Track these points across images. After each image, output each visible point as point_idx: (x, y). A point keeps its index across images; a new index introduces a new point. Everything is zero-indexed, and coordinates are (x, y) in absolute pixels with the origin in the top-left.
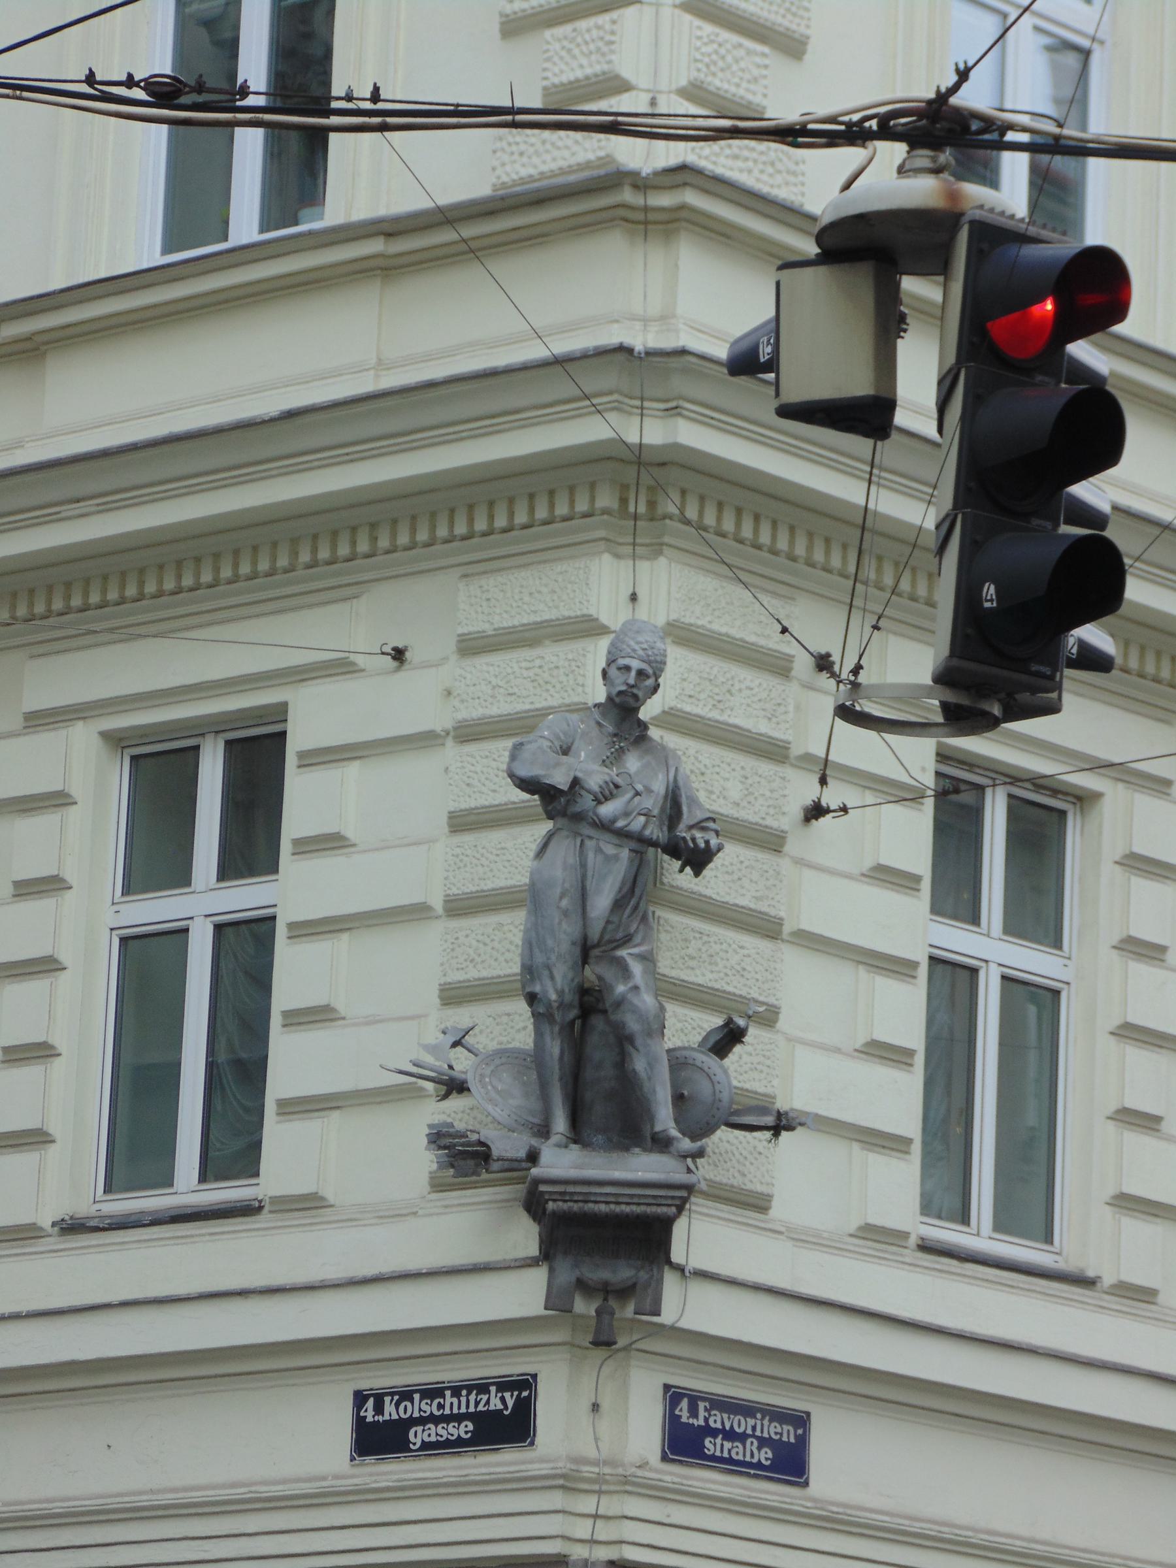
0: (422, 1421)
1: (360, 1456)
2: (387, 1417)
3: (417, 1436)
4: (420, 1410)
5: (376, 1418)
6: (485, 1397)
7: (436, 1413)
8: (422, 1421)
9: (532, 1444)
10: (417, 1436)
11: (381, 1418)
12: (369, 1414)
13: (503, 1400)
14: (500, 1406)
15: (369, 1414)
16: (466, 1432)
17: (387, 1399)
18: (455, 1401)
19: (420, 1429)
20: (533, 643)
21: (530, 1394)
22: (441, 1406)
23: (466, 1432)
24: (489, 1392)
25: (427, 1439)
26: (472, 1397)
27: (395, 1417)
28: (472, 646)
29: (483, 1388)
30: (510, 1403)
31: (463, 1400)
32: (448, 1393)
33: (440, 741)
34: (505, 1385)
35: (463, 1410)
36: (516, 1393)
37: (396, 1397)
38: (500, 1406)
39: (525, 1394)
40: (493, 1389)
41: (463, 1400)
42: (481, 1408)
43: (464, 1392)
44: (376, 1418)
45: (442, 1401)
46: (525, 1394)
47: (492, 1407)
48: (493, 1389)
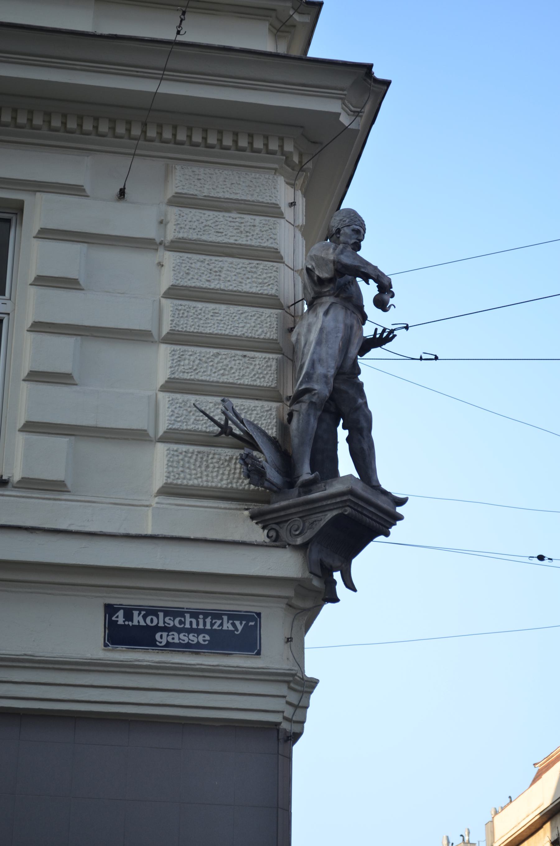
0: (166, 629)
1: (112, 644)
2: (135, 623)
3: (162, 638)
4: (164, 622)
5: (127, 623)
6: (219, 622)
7: (178, 625)
8: (166, 629)
9: (259, 653)
10: (162, 638)
11: (130, 623)
12: (120, 618)
13: (234, 625)
14: (231, 628)
15: (120, 618)
16: (204, 641)
17: (136, 613)
18: (194, 621)
19: (164, 634)
20: (227, 210)
21: (256, 624)
22: (181, 622)
23: (204, 641)
24: (222, 619)
25: (170, 640)
26: (208, 620)
27: (142, 623)
28: (180, 201)
29: (217, 615)
30: (240, 628)
31: (201, 621)
32: (187, 616)
33: (155, 247)
34: (233, 616)
35: (201, 626)
36: (244, 622)
37: (143, 613)
38: (231, 628)
39: (252, 623)
40: (225, 618)
41: (201, 621)
42: (215, 627)
43: (201, 616)
44: (127, 623)
45: (183, 619)
46: (252, 623)
47: (225, 628)
48: (225, 618)
